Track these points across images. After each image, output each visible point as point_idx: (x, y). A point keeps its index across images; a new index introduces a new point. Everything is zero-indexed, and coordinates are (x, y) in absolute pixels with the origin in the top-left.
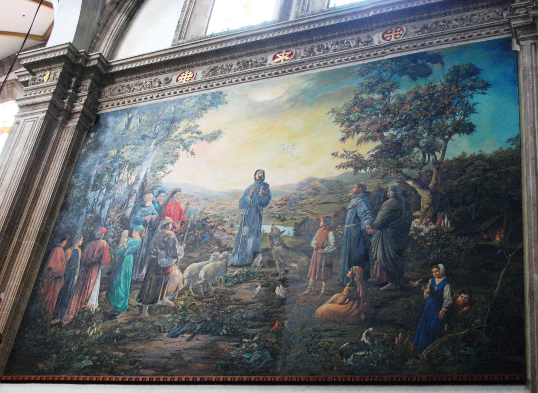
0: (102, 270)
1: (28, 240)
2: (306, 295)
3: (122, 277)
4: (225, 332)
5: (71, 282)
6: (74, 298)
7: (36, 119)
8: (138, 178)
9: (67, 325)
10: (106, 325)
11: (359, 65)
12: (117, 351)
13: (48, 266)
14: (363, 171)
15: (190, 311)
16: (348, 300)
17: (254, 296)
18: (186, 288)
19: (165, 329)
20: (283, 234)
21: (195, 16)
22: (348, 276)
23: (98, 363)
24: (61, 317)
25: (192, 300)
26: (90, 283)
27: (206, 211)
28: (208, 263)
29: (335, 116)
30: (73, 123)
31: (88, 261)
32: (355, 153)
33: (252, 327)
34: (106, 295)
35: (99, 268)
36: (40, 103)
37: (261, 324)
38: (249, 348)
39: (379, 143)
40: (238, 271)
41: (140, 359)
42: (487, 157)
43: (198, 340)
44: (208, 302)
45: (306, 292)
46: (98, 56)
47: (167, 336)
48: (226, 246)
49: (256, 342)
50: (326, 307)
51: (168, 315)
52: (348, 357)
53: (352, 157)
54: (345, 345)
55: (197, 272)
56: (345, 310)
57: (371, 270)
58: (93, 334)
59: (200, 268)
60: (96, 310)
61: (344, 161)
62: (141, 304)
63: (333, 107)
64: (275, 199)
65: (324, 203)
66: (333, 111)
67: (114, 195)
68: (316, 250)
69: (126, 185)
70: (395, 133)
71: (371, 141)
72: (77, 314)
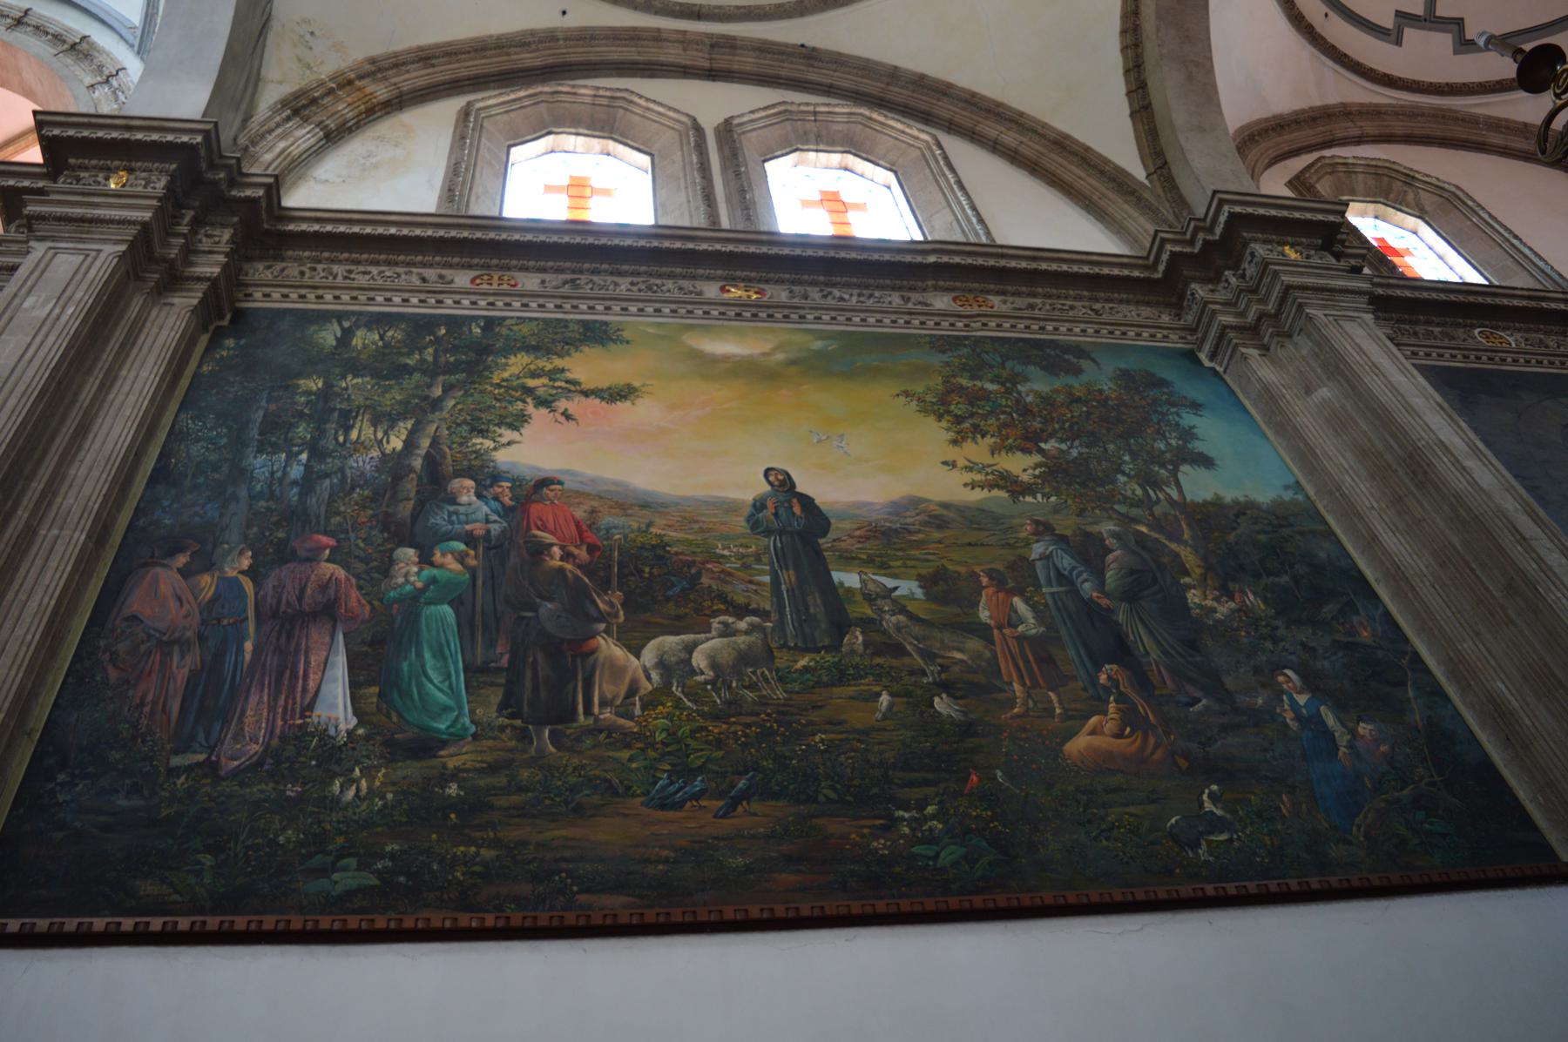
0: (345, 635)
1: (61, 529)
2: (1018, 716)
3: (427, 655)
4: (833, 795)
5: (230, 659)
6: (254, 699)
7: (94, 254)
8: (410, 444)
9: (236, 773)
10: (401, 773)
11: (926, 335)
12: (468, 845)
13: (126, 612)
14: (1029, 499)
15: (694, 744)
16: (1128, 729)
17: (879, 715)
18: (664, 689)
19: (628, 788)
20: (897, 593)
21: (478, 198)
22: (1101, 682)
23: (402, 879)
24: (211, 749)
25: (690, 719)
26: (307, 663)
27: (653, 530)
28: (708, 639)
29: (915, 402)
30: (184, 302)
31: (283, 608)
32: (995, 468)
33: (911, 784)
34: (380, 695)
35: (334, 627)
36: (111, 221)
37: (930, 776)
38: (923, 832)
39: (1037, 458)
40: (807, 659)
41: (564, 865)
42: (1265, 506)
43: (755, 814)
44: (748, 726)
45: (1016, 710)
46: (271, 180)
47: (642, 804)
48: (749, 605)
49: (933, 817)
50: (1079, 744)
51: (625, 754)
52: (1195, 846)
53: (992, 473)
54: (1173, 821)
55: (683, 655)
56: (1134, 748)
57: (1150, 673)
58: (357, 795)
59: (690, 648)
60: (350, 733)
61: (978, 477)
62: (518, 722)
63: (903, 388)
64: (838, 528)
65: (970, 544)
66: (907, 394)
67: (342, 470)
68: (1000, 628)
69: (375, 453)
70: (1064, 447)
71: (1019, 454)
72: (275, 742)
